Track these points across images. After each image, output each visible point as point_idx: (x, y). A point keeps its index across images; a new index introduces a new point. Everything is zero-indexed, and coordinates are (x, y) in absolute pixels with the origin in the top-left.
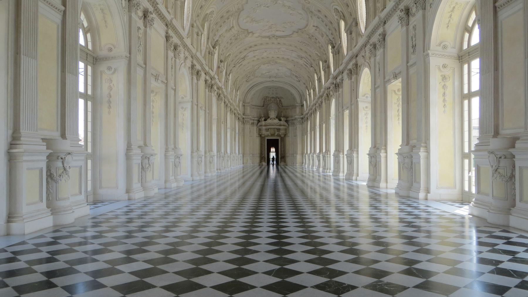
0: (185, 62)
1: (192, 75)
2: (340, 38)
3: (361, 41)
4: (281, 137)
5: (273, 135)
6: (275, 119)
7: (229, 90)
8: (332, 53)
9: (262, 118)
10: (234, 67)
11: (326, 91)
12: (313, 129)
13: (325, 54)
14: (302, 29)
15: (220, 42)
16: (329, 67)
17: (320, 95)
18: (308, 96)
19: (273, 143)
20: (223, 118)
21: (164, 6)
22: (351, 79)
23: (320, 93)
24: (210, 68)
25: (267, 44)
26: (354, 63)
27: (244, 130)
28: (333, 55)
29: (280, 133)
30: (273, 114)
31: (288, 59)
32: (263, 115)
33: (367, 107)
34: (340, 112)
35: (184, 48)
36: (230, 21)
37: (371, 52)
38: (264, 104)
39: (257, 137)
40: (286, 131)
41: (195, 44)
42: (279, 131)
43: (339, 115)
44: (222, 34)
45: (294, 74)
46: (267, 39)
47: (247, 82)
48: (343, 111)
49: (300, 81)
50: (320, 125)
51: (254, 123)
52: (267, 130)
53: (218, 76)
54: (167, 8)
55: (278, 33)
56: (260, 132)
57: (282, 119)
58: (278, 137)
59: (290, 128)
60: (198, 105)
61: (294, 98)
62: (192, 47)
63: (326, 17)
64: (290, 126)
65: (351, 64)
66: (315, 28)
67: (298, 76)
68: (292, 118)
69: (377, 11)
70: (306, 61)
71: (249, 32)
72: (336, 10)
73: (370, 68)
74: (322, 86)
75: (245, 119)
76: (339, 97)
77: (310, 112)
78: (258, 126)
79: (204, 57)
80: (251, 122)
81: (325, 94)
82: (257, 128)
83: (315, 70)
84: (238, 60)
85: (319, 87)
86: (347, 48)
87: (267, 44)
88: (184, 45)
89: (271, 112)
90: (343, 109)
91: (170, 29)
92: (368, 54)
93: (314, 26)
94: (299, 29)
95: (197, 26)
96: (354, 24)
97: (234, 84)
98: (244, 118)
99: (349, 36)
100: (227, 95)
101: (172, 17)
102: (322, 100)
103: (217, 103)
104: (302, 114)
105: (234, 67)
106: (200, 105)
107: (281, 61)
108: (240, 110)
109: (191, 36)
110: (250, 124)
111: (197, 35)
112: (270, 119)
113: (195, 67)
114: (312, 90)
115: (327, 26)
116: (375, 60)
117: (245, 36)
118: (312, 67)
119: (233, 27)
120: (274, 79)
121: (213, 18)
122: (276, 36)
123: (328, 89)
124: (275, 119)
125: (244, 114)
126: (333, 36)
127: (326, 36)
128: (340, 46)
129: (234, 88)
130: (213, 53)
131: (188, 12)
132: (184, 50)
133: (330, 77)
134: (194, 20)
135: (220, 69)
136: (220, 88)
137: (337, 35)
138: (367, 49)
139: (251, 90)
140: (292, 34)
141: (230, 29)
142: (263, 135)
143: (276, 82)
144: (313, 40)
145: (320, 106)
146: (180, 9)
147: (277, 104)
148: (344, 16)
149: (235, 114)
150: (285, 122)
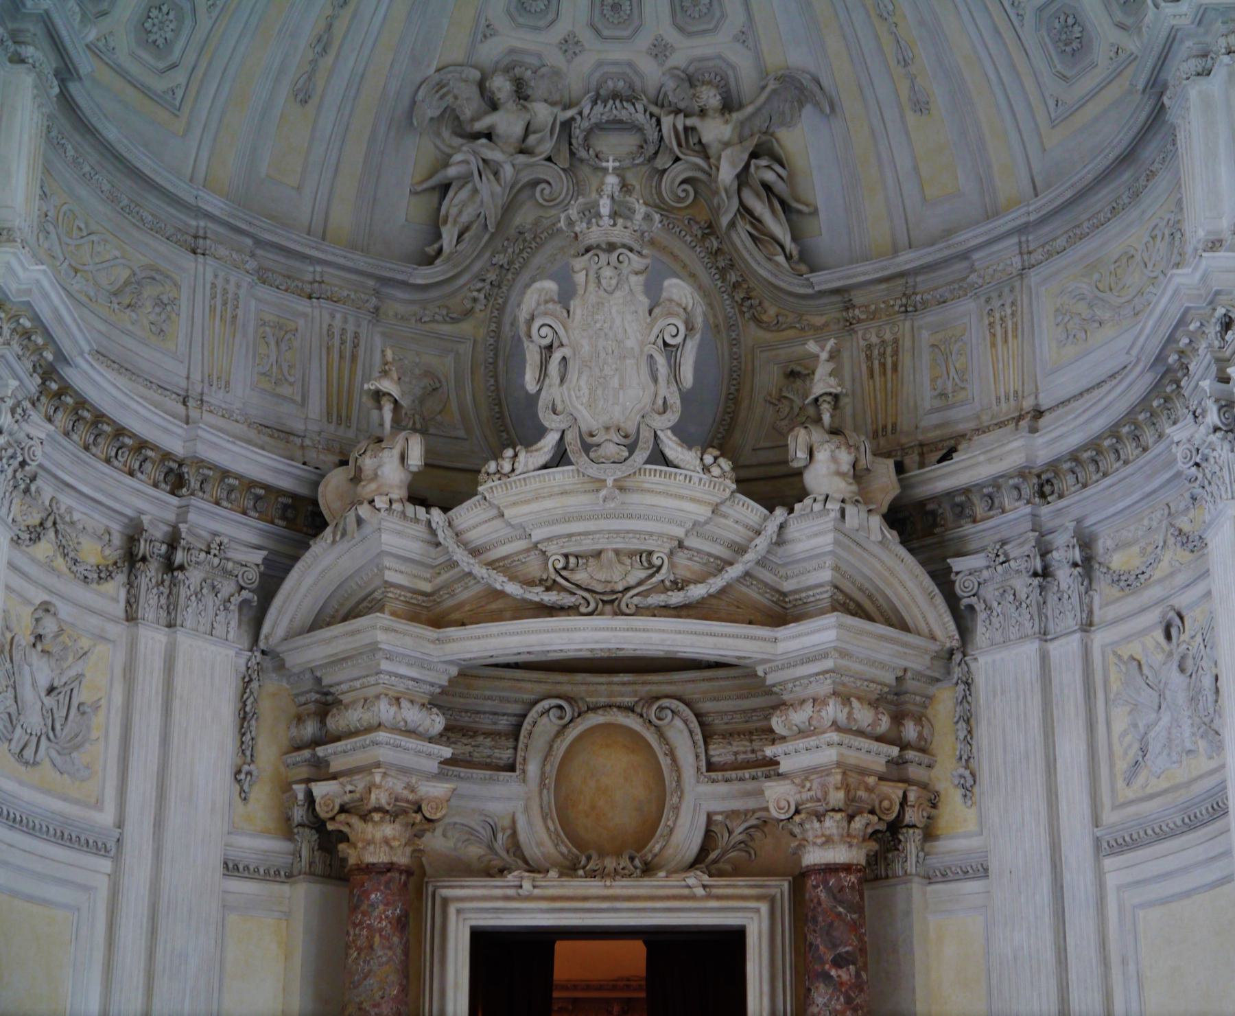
4: (800, 878)
6: (659, 457)
51: (173, 541)
56: (320, 770)
58: (741, 886)
64: (982, 633)
82: (247, 683)
89: (566, 296)
110: (92, 552)
112: (560, 458)
142: (389, 830)
147: (710, 229)
150: (876, 521)
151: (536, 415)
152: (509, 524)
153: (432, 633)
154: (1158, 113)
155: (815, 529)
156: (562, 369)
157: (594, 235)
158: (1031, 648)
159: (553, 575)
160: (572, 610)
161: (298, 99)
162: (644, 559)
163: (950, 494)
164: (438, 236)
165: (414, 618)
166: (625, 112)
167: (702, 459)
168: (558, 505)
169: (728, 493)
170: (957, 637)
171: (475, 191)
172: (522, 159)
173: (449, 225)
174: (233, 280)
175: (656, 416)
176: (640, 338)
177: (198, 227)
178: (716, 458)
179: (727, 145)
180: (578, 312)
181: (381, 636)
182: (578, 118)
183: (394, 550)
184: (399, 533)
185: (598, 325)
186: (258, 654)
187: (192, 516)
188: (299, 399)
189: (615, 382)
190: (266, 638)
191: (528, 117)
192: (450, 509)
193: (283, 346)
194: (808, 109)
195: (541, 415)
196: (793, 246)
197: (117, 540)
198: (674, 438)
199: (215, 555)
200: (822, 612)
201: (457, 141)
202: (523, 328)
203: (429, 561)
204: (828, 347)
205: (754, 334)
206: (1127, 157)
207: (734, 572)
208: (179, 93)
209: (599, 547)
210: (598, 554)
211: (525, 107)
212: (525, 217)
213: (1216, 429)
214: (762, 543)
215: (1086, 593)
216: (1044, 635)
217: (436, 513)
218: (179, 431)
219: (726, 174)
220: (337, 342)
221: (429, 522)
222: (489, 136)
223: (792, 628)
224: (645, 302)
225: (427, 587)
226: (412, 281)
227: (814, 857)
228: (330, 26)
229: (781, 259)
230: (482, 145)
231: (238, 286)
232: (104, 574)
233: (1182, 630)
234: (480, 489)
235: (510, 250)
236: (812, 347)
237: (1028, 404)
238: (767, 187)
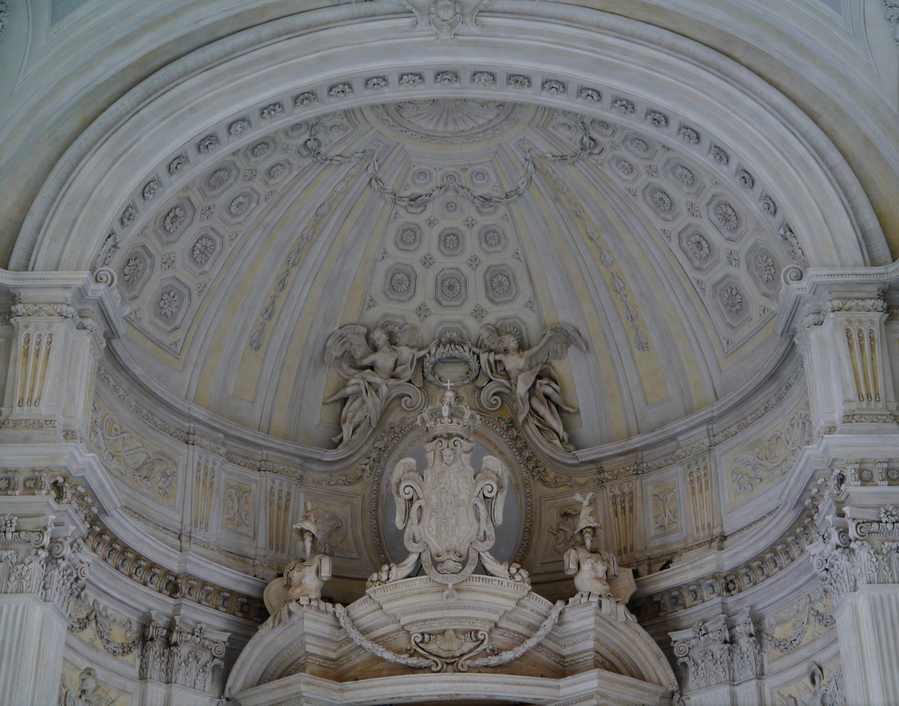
6: (482, 569)
51: (170, 628)
64: (692, 681)
89: (421, 467)
110: (119, 635)
112: (418, 571)
139: (134, 112)
147: (512, 424)
150: (622, 609)
151: (402, 543)
152: (385, 614)
153: (336, 685)
154: (792, 346)
155: (583, 614)
156: (419, 514)
157: (439, 429)
158: (725, 690)
159: (415, 647)
160: (426, 669)
161: (254, 346)
162: (473, 635)
163: (669, 590)
164: (341, 431)
165: (325, 675)
166: (457, 352)
167: (509, 570)
168: (417, 601)
169: (526, 592)
170: (676, 683)
171: (364, 402)
172: (393, 382)
173: (347, 424)
174: (211, 460)
175: (479, 543)
176: (469, 493)
177: (189, 427)
178: (518, 570)
179: (521, 371)
180: (429, 477)
181: (303, 688)
182: (428, 356)
183: (312, 632)
184: (315, 620)
185: (442, 486)
186: (224, 700)
187: (183, 611)
188: (252, 534)
189: (453, 522)
190: (230, 689)
191: (396, 355)
192: (348, 604)
193: (242, 501)
194: (572, 349)
195: (406, 543)
196: (565, 433)
197: (135, 627)
198: (491, 557)
199: (197, 636)
200: (588, 669)
201: (355, 371)
202: (394, 488)
203: (334, 638)
204: (588, 498)
205: (540, 489)
206: (773, 376)
207: (531, 643)
208: (180, 344)
209: (444, 628)
210: (443, 632)
211: (394, 350)
212: (395, 417)
213: (838, 547)
214: (548, 624)
215: (759, 653)
216: (732, 682)
217: (339, 607)
218: (176, 556)
219: (522, 389)
220: (276, 498)
221: (334, 613)
222: (372, 368)
223: (569, 680)
224: (472, 471)
225: (333, 655)
226: (324, 459)
228: (273, 302)
229: (557, 442)
230: (368, 374)
231: (214, 464)
232: (126, 649)
233: (822, 677)
234: (367, 591)
235: (386, 439)
236: (578, 497)
237: (717, 531)
238: (547, 397)
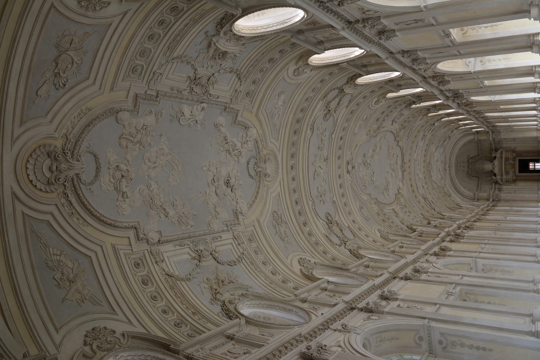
0: (432, 263)
1: (445, 256)
2: (405, 96)
3: (409, 74)
4: (516, 156)
5: (513, 166)
6: (494, 164)
7: (460, 216)
8: (420, 103)
9: (492, 178)
10: (434, 209)
11: (462, 107)
12: (505, 119)
13: (421, 110)
14: (395, 136)
15: (408, 223)
16: (435, 106)
17: (466, 114)
18: (466, 127)
19: (524, 166)
20: (494, 225)
21: (375, 279)
22: (449, 81)
23: (464, 113)
24: (437, 236)
25: (410, 173)
26: (432, 80)
27: (507, 201)
28: (422, 102)
29: (511, 157)
30: (488, 166)
31: (426, 150)
32: (489, 178)
33: (481, 61)
34: (486, 90)
35: (417, 262)
36: (387, 212)
37: (420, 63)
38: (476, 177)
39: (516, 185)
40: (508, 151)
41: (411, 251)
42: (509, 159)
43: (491, 91)
44: (401, 222)
45: (441, 143)
46: (405, 173)
47: (450, 195)
48: (485, 87)
49: (450, 137)
50: (502, 112)
52: (507, 173)
53: (445, 228)
54: (377, 277)
55: (399, 162)
56: (510, 181)
57: (494, 155)
59: (504, 146)
60: (479, 252)
61: (469, 142)
62: (416, 254)
63: (383, 113)
65: (432, 82)
66: (394, 123)
67: (444, 138)
68: (492, 144)
69: (379, 61)
70: (428, 131)
71: (398, 192)
72: (377, 102)
73: (438, 62)
74: (456, 112)
75: (494, 199)
76: (469, 92)
77: (485, 123)
78: (501, 183)
79: (425, 242)
80: (497, 192)
81: (465, 108)
82: (505, 185)
83: (438, 120)
84: (427, 205)
85: (456, 115)
86: (416, 88)
87: (410, 173)
88: (414, 262)
89: (485, 169)
90: (483, 87)
91: (399, 275)
92: (422, 67)
93: (392, 124)
94: (395, 140)
95: (393, 247)
96: (391, 84)
97: (454, 210)
98: (493, 200)
99: (403, 87)
100: (467, 219)
101: (386, 271)
102: (472, 111)
103: (476, 230)
104: (488, 132)
105: (434, 209)
106: (480, 250)
107: (428, 158)
108: (484, 205)
109: (404, 254)
110: (500, 192)
111: (403, 247)
112: (494, 169)
113: (437, 252)
114: (460, 123)
115: (392, 111)
116: (429, 58)
117: (402, 197)
118: (434, 124)
119: (393, 210)
120: (447, 165)
121: (384, 230)
122: (402, 163)
123: (459, 105)
124: (494, 164)
125: (488, 200)
126: (403, 104)
127: (402, 111)
128: (413, 95)
129: (458, 210)
130: (420, 232)
131: (380, 255)
132: (419, 262)
133: (446, 104)
134: (386, 249)
135: (438, 225)
136: (458, 226)
137: (402, 100)
138: (416, 68)
140: (400, 147)
141: (395, 212)
142: (514, 177)
143: (450, 163)
144: (406, 125)
145: (478, 112)
146: (377, 264)
148: (382, 94)
149: (488, 211)
150: (497, 153)
227: (515, 155)
